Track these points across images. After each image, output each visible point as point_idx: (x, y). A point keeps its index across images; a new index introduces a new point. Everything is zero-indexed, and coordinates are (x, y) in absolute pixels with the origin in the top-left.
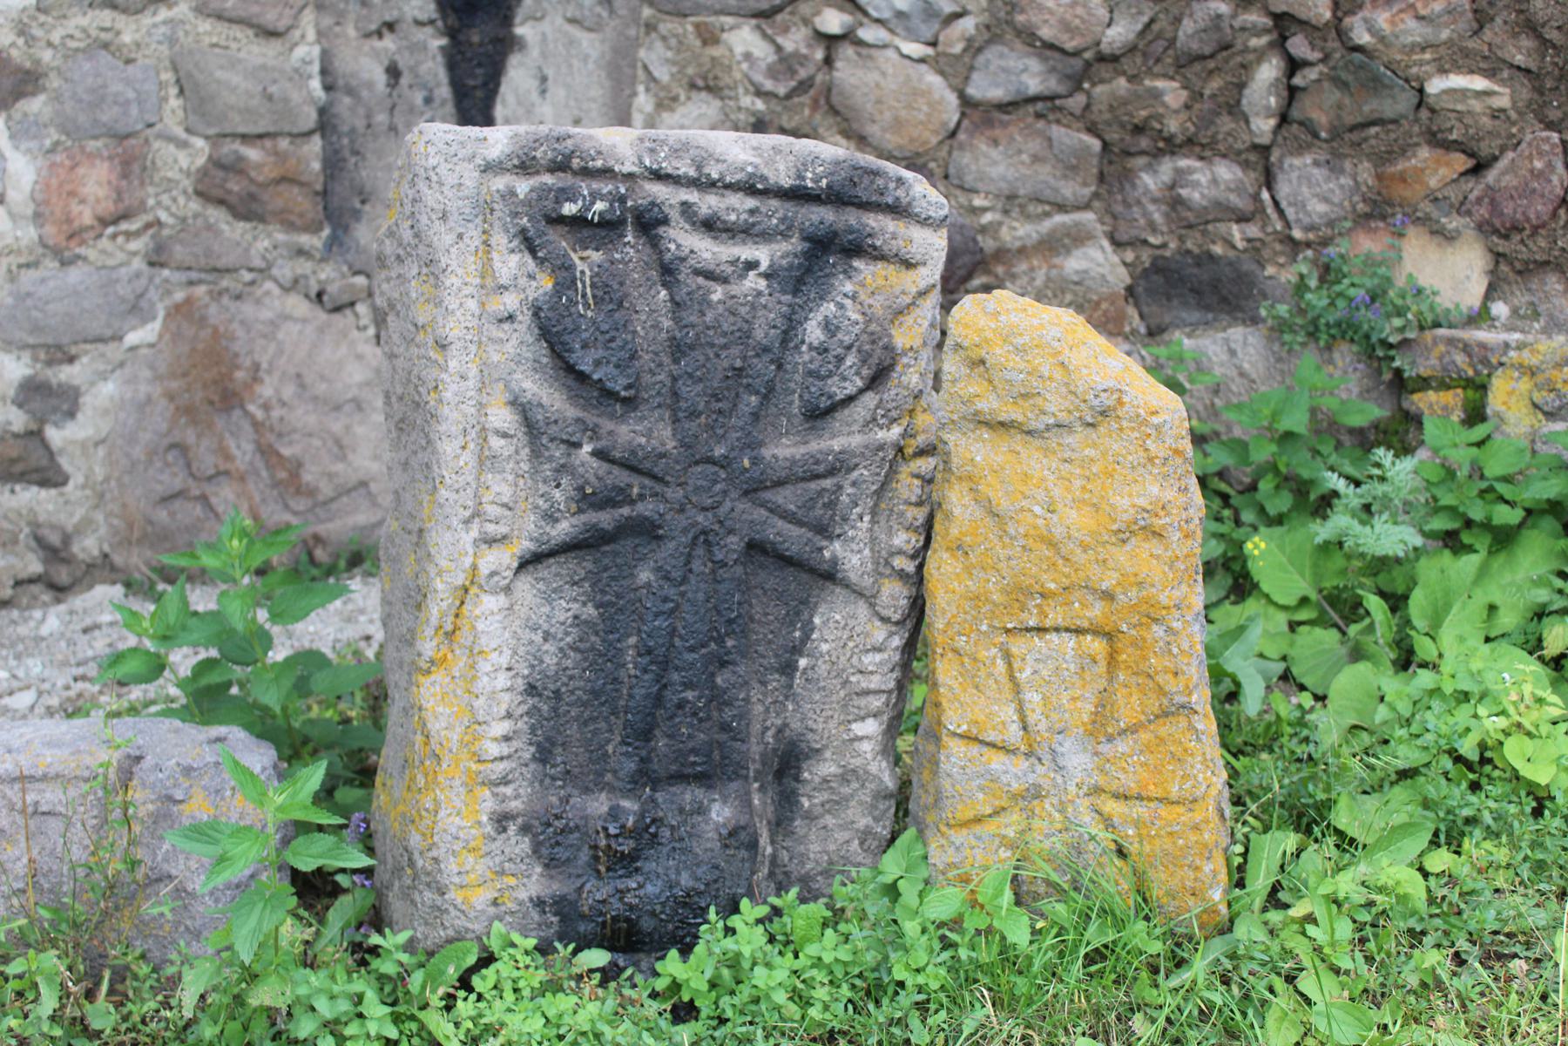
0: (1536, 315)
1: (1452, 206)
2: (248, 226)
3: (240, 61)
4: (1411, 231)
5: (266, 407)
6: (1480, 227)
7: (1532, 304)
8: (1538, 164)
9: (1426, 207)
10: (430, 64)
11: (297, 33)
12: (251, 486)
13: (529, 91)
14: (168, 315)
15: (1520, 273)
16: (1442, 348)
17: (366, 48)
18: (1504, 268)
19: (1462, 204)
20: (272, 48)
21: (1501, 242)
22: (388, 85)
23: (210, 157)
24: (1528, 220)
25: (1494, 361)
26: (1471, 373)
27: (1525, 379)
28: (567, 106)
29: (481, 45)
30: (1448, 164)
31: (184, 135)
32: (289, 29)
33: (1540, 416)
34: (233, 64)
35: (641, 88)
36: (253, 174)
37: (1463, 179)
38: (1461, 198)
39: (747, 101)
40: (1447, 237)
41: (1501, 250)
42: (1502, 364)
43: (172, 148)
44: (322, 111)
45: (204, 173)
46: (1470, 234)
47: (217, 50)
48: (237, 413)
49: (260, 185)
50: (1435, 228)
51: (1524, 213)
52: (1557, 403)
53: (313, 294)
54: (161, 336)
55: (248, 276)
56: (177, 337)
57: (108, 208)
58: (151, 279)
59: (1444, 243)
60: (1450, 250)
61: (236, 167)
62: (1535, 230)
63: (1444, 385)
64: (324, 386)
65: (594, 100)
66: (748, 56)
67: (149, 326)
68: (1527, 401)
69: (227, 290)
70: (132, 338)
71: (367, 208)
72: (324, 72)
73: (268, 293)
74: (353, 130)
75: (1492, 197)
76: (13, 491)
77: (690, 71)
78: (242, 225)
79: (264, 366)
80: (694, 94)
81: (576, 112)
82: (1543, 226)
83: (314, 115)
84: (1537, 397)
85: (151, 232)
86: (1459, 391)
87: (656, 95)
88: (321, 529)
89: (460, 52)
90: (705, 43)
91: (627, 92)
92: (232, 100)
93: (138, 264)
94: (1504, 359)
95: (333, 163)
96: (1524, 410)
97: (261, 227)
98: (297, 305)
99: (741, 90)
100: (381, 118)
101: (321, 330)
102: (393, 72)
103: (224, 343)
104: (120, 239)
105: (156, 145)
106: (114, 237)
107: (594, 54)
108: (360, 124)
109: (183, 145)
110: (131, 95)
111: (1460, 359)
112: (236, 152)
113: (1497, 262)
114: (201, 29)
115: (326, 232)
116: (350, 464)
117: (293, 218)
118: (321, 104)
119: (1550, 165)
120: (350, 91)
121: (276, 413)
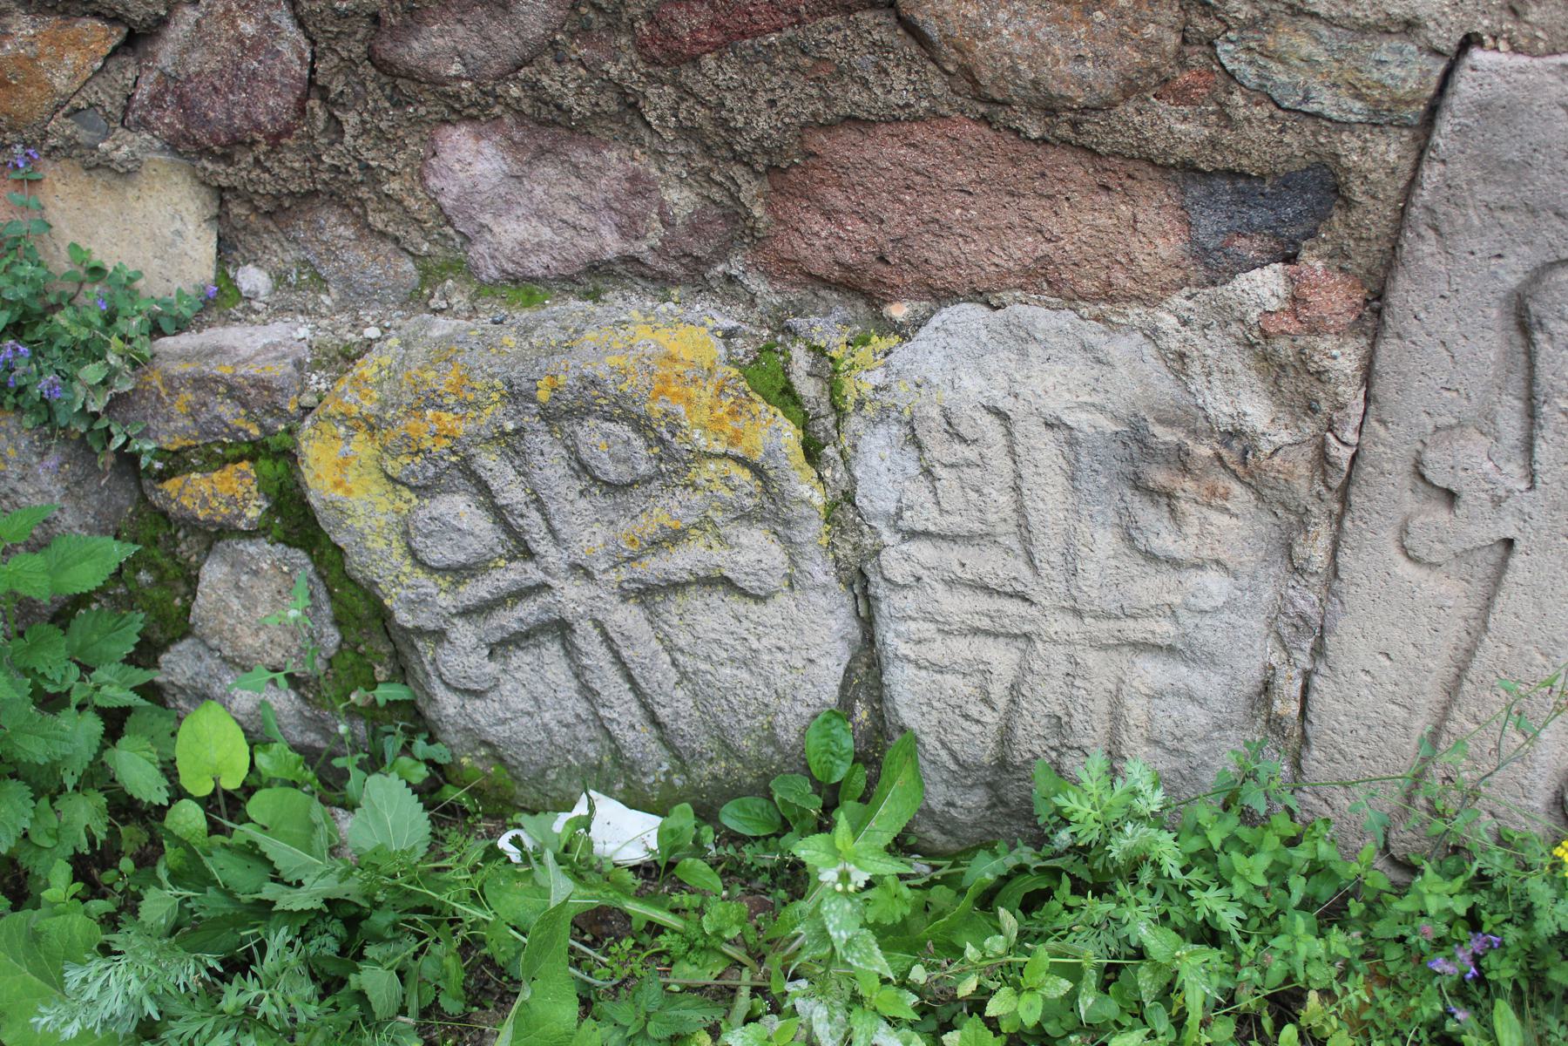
0: (320, 282)
1: (108, 117)
4: (50, 171)
6: (174, 145)
7: (306, 262)
8: (248, 28)
9: (61, 127)
15: (269, 214)
16: (188, 396)
18: (238, 210)
19: (126, 109)
21: (221, 167)
24: (258, 126)
25: (291, 408)
26: (255, 432)
27: (361, 436)
30: (76, 43)
33: (407, 494)
37: (112, 65)
38: (120, 100)
40: (124, 173)
41: (224, 182)
42: (308, 410)
46: (159, 159)
50: (93, 160)
51: (247, 116)
52: (431, 471)
59: (118, 182)
60: (131, 193)
62: (275, 140)
63: (214, 460)
68: (376, 475)
75: (175, 90)
82: (288, 131)
84: (392, 466)
86: (245, 466)
94: (308, 400)
96: (375, 489)
111: (227, 410)
113: (223, 203)
119: (268, 24)
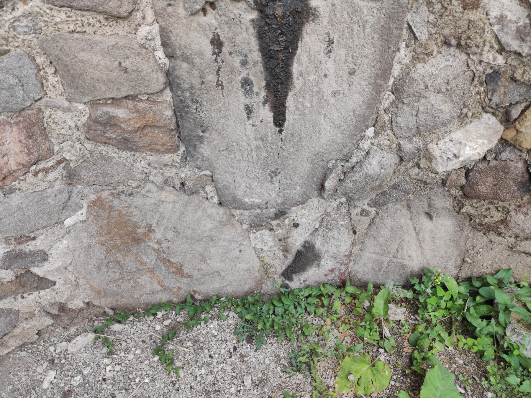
2: (129, 154)
3: (96, 43)
5: (158, 242)
10: (245, 35)
11: (138, 15)
12: (157, 273)
13: (318, 52)
14: (89, 206)
17: (195, 24)
20: (122, 28)
22: (214, 53)
23: (90, 116)
28: (346, 61)
29: (283, 17)
31: (66, 104)
32: (130, 13)
34: (91, 46)
35: (403, 45)
36: (123, 126)
39: (489, 56)
43: (60, 113)
44: (168, 73)
45: (88, 127)
47: (76, 35)
48: (143, 245)
49: (131, 132)
53: (178, 185)
54: (88, 218)
55: (135, 184)
56: (97, 217)
57: (23, 158)
58: (70, 192)
61: (110, 122)
64: (190, 232)
65: (367, 57)
66: (501, 19)
67: (79, 212)
69: (123, 192)
70: (68, 222)
71: (207, 135)
72: (164, 45)
73: (149, 191)
74: (192, 87)
76: (23, 297)
77: (447, 32)
78: (124, 154)
79: (154, 225)
80: (444, 49)
81: (352, 66)
83: (162, 78)
85: (62, 165)
87: (414, 51)
88: (197, 288)
89: (267, 24)
90: (465, 7)
91: (393, 49)
92: (97, 74)
93: (58, 186)
95: (180, 110)
97: (137, 154)
98: (169, 196)
99: (487, 48)
100: (211, 77)
101: (185, 205)
102: (217, 43)
103: (127, 218)
104: (40, 175)
105: (47, 113)
106: (36, 174)
107: (372, 20)
108: (196, 82)
109: (67, 110)
110: (13, 81)
112: (107, 113)
114: (58, 20)
115: (183, 149)
116: (209, 265)
117: (157, 147)
118: (166, 68)
120: (186, 59)
121: (165, 245)
